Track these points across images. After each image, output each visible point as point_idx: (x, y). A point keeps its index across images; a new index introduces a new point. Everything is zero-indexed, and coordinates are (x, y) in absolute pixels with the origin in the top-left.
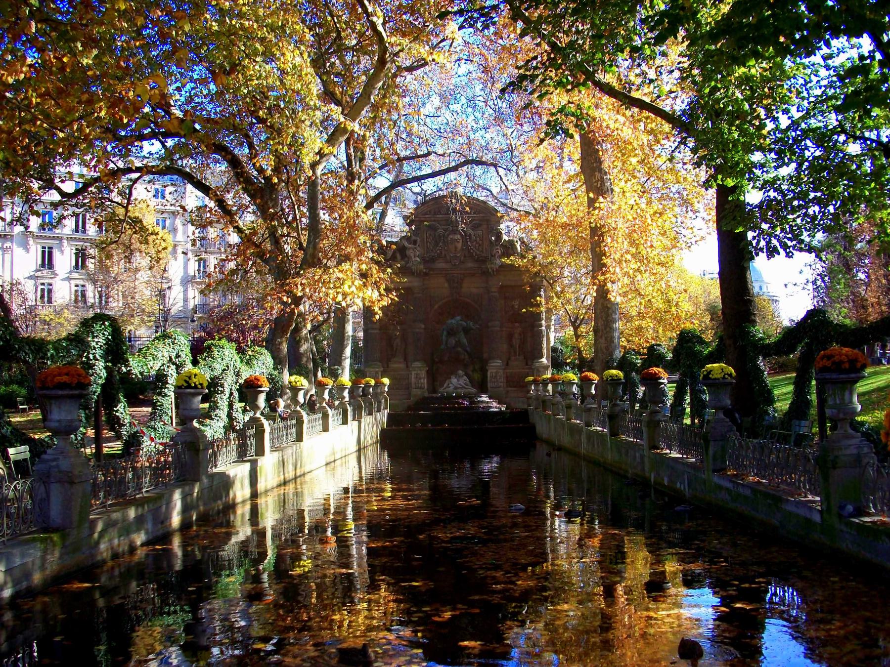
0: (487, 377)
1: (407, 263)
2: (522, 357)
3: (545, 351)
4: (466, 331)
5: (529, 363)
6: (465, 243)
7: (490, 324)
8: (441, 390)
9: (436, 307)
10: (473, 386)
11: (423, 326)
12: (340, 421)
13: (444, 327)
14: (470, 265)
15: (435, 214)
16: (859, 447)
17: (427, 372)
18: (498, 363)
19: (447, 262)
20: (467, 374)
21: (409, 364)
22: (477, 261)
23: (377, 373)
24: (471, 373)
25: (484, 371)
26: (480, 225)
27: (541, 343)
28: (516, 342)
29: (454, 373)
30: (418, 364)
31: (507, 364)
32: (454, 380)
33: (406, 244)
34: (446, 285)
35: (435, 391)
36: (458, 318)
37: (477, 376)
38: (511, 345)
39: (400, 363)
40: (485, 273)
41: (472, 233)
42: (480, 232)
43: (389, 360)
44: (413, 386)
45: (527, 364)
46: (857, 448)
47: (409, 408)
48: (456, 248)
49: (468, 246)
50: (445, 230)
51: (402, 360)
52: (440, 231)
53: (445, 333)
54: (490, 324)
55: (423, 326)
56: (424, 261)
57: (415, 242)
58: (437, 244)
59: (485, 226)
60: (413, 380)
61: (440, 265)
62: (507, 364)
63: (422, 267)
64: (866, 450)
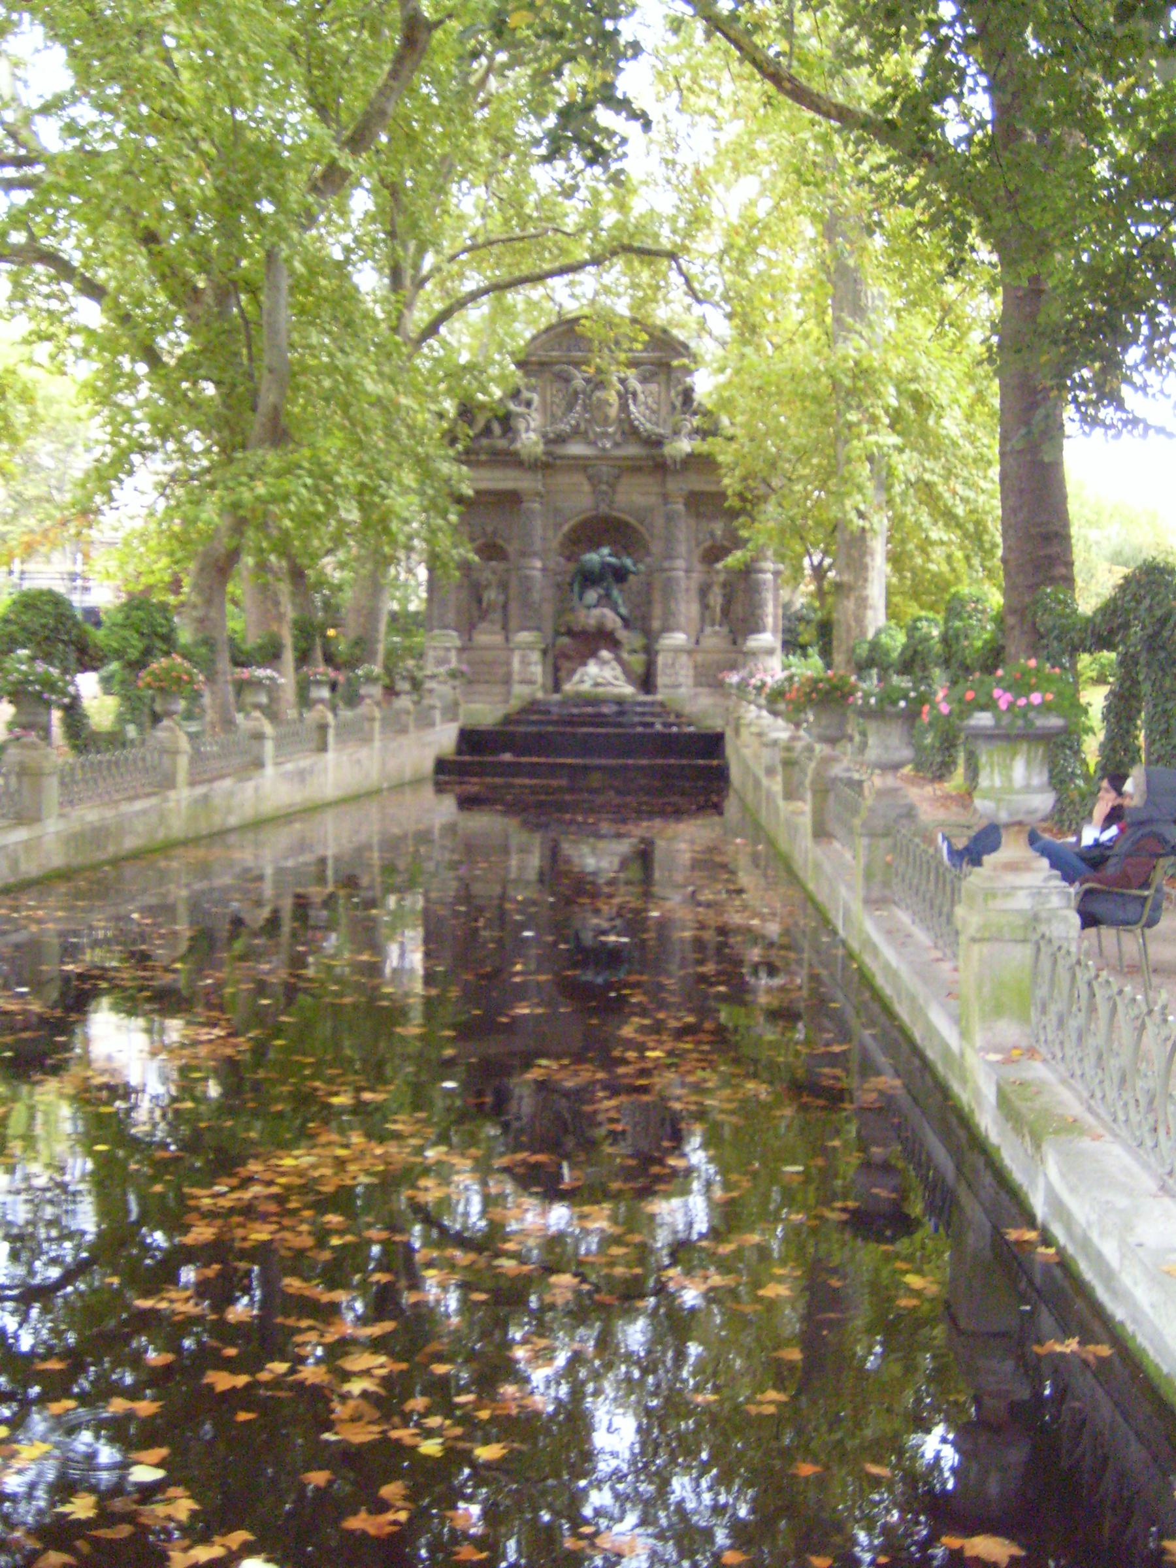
1: (513, 440)
2: (725, 630)
3: (770, 621)
4: (620, 575)
6: (624, 407)
7: (666, 564)
8: (568, 687)
9: (566, 528)
11: (538, 564)
12: (313, 745)
14: (633, 450)
16: (1038, 894)
17: (544, 652)
18: (679, 638)
20: (619, 660)
23: (448, 649)
24: (625, 656)
25: (650, 652)
26: (654, 374)
27: (761, 605)
28: (716, 599)
29: (593, 654)
30: (524, 637)
31: (697, 642)
32: (592, 668)
33: (512, 406)
34: (587, 488)
35: (557, 688)
36: (605, 551)
37: (637, 661)
38: (705, 606)
39: (493, 633)
40: (661, 467)
41: (639, 387)
42: (653, 387)
43: (472, 626)
44: (516, 677)
45: (735, 643)
46: (1033, 895)
47: (507, 720)
48: (606, 417)
49: (629, 413)
51: (498, 627)
52: (578, 383)
54: (666, 564)
56: (548, 441)
57: (528, 404)
58: (570, 407)
60: (516, 665)
61: (576, 449)
64: (1055, 901)
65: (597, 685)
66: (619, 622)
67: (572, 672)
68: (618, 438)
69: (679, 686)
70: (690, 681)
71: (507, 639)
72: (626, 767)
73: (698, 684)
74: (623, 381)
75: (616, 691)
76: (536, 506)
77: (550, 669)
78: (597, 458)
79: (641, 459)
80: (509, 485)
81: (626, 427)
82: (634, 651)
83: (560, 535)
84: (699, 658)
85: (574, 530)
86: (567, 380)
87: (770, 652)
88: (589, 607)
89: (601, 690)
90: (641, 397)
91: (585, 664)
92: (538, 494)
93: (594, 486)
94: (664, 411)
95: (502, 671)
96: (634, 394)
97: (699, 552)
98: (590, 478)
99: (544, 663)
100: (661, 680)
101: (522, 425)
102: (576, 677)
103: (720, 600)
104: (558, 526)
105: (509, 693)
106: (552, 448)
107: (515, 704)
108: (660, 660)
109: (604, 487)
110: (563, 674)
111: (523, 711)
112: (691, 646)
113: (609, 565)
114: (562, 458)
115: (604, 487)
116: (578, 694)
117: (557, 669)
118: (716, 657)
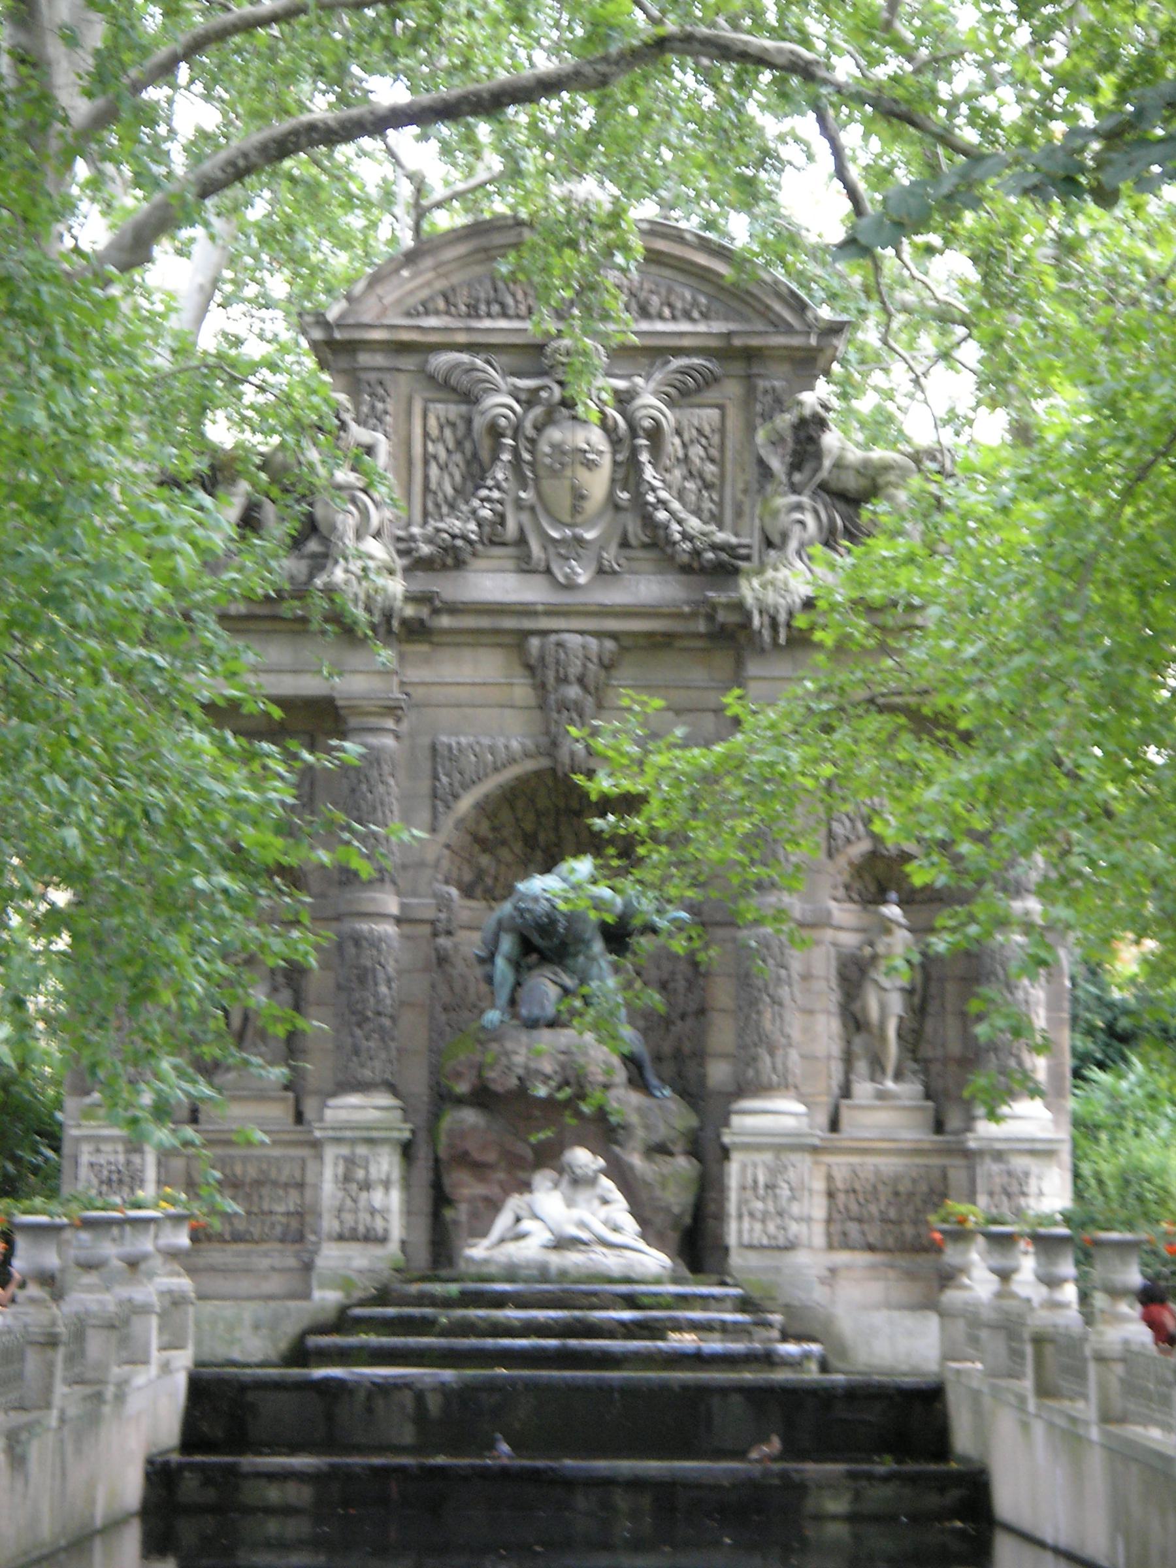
0: (722, 1189)
1: (320, 562)
2: (909, 1090)
5: (954, 1121)
8: (478, 1251)
9: (466, 804)
10: (649, 1230)
11: (392, 905)
13: (507, 907)
15: (473, 311)
17: (407, 1150)
19: (525, 566)
21: (310, 1106)
22: (686, 569)
24: (636, 1160)
26: (710, 381)
31: (834, 1125)
34: (522, 692)
41: (669, 419)
44: (329, 1224)
45: (939, 1127)
48: (579, 496)
50: (529, 400)
53: (507, 944)
55: (392, 905)
56: (418, 565)
59: (732, 389)
60: (329, 1189)
62: (834, 1125)
63: (396, 586)
65: (562, 1243)
66: (621, 1075)
67: (494, 1206)
68: (610, 555)
69: (790, 1246)
70: (819, 1240)
71: (299, 1118)
72: (569, 1483)
73: (837, 1241)
74: (623, 399)
75: (611, 1262)
76: (389, 741)
77: (423, 1201)
78: (552, 612)
79: (679, 616)
80: (309, 685)
81: (633, 527)
82: (659, 1150)
83: (448, 823)
84: (841, 1165)
85: (483, 808)
86: (469, 398)
87: (1043, 1152)
88: (532, 1024)
89: (573, 1259)
90: (673, 445)
91: (525, 1187)
92: (392, 710)
93: (541, 687)
94: (737, 480)
95: (283, 1205)
96: (655, 434)
97: (839, 870)
98: (530, 668)
99: (407, 1184)
100: (735, 1232)
101: (347, 521)
102: (503, 1222)
103: (896, 1004)
104: (440, 799)
105: (308, 1267)
106: (425, 582)
107: (327, 1297)
108: (734, 1169)
109: (573, 692)
110: (460, 1213)
111: (342, 1322)
112: (819, 1133)
113: (598, 904)
114: (453, 609)
115: (573, 692)
116: (511, 1273)
117: (440, 1198)
118: (889, 1165)
